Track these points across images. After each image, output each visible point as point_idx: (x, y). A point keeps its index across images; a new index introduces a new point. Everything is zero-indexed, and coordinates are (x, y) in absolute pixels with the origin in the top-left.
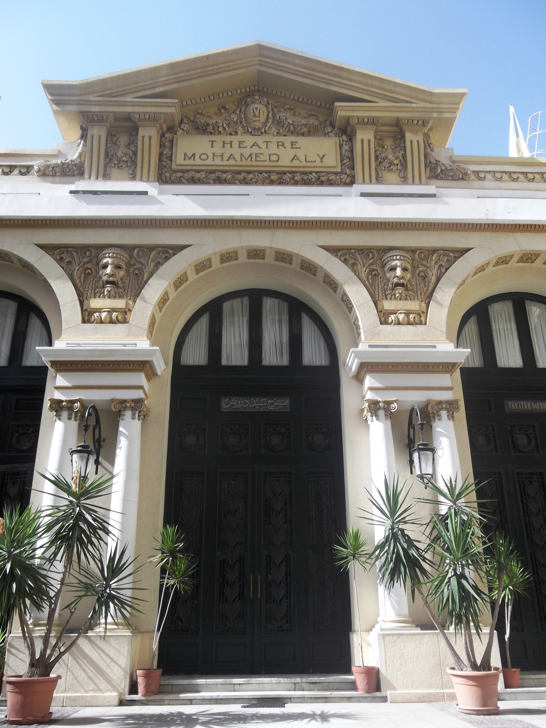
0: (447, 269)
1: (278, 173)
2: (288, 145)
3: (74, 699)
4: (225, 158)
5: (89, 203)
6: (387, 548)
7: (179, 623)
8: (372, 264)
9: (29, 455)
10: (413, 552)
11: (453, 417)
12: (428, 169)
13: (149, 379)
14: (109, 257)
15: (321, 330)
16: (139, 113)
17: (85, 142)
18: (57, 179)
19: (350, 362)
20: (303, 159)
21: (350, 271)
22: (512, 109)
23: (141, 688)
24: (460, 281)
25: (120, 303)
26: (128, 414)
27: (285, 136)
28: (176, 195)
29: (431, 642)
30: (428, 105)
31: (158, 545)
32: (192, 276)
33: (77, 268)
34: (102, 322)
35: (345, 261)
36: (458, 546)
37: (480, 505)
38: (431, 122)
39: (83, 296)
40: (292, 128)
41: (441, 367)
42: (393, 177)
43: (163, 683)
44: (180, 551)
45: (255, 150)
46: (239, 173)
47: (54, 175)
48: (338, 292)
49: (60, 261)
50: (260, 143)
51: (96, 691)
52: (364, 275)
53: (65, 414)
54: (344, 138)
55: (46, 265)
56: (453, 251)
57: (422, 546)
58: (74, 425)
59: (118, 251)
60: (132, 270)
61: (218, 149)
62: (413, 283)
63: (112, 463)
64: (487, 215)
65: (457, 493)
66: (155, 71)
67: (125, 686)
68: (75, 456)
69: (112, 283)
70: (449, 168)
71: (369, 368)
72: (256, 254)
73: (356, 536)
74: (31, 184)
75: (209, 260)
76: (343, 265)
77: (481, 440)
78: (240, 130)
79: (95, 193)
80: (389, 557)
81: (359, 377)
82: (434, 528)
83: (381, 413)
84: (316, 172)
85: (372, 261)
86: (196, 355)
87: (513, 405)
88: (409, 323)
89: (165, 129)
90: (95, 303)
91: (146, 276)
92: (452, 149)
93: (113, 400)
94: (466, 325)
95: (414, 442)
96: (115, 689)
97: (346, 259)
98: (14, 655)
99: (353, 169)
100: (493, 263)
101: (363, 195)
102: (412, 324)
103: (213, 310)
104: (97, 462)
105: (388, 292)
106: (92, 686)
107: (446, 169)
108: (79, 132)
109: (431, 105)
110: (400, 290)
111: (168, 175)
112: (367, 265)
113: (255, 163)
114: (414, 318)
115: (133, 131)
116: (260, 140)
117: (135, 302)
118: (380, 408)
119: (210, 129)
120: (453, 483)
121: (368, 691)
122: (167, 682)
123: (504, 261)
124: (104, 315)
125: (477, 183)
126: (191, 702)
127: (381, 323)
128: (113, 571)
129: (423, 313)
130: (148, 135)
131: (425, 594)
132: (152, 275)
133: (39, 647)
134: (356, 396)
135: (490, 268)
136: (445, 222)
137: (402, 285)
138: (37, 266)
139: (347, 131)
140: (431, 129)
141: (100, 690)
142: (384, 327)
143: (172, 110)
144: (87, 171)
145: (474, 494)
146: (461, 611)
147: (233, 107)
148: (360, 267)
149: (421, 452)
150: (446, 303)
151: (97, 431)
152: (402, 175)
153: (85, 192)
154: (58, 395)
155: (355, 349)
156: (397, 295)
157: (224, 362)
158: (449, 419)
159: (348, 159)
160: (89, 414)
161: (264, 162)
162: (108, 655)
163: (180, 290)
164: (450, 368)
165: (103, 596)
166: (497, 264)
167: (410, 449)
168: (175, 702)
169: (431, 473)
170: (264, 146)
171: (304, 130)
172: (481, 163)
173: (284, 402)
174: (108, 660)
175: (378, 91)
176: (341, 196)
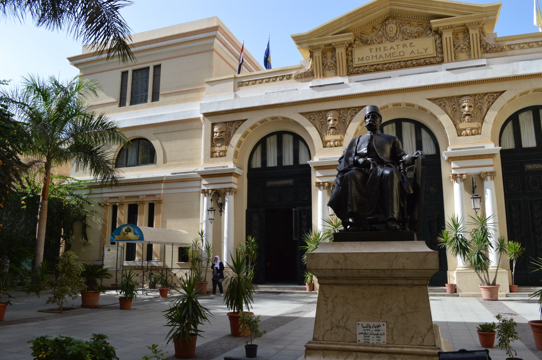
0: (492, 103)
2: (408, 45)
4: (378, 58)
5: (318, 91)
8: (454, 105)
12: (482, 49)
16: (335, 43)
17: (313, 59)
18: (303, 80)
19: (444, 156)
20: (416, 52)
24: (499, 109)
25: (338, 137)
27: (407, 39)
28: (357, 82)
30: (480, 14)
34: (331, 147)
38: (482, 23)
40: (410, 35)
42: (463, 55)
45: (392, 51)
46: (385, 64)
49: (310, 119)
50: (394, 46)
53: (322, 187)
54: (437, 36)
58: (326, 191)
61: (374, 53)
66: (340, 20)
69: (333, 128)
70: (493, 46)
79: (321, 86)
83: (459, 179)
84: (423, 58)
87: (529, 167)
88: (472, 135)
89: (348, 46)
90: (328, 138)
91: (348, 123)
94: (506, 127)
99: (443, 53)
101: (447, 70)
107: (492, 47)
108: (308, 54)
109: (482, 14)
110: (467, 118)
111: (352, 70)
113: (392, 58)
115: (334, 50)
116: (394, 44)
119: (369, 42)
125: (510, 53)
127: (459, 136)
130: (341, 51)
134: (448, 170)
137: (469, 115)
138: (301, 123)
139: (438, 33)
140: (484, 24)
142: (459, 137)
144: (315, 74)
150: (493, 118)
152: (468, 54)
153: (316, 86)
154: (318, 180)
155: (445, 152)
158: (491, 180)
159: (440, 48)
166: (521, 95)
170: (396, 48)
171: (416, 35)
172: (512, 40)
175: (453, 10)
176: (436, 71)
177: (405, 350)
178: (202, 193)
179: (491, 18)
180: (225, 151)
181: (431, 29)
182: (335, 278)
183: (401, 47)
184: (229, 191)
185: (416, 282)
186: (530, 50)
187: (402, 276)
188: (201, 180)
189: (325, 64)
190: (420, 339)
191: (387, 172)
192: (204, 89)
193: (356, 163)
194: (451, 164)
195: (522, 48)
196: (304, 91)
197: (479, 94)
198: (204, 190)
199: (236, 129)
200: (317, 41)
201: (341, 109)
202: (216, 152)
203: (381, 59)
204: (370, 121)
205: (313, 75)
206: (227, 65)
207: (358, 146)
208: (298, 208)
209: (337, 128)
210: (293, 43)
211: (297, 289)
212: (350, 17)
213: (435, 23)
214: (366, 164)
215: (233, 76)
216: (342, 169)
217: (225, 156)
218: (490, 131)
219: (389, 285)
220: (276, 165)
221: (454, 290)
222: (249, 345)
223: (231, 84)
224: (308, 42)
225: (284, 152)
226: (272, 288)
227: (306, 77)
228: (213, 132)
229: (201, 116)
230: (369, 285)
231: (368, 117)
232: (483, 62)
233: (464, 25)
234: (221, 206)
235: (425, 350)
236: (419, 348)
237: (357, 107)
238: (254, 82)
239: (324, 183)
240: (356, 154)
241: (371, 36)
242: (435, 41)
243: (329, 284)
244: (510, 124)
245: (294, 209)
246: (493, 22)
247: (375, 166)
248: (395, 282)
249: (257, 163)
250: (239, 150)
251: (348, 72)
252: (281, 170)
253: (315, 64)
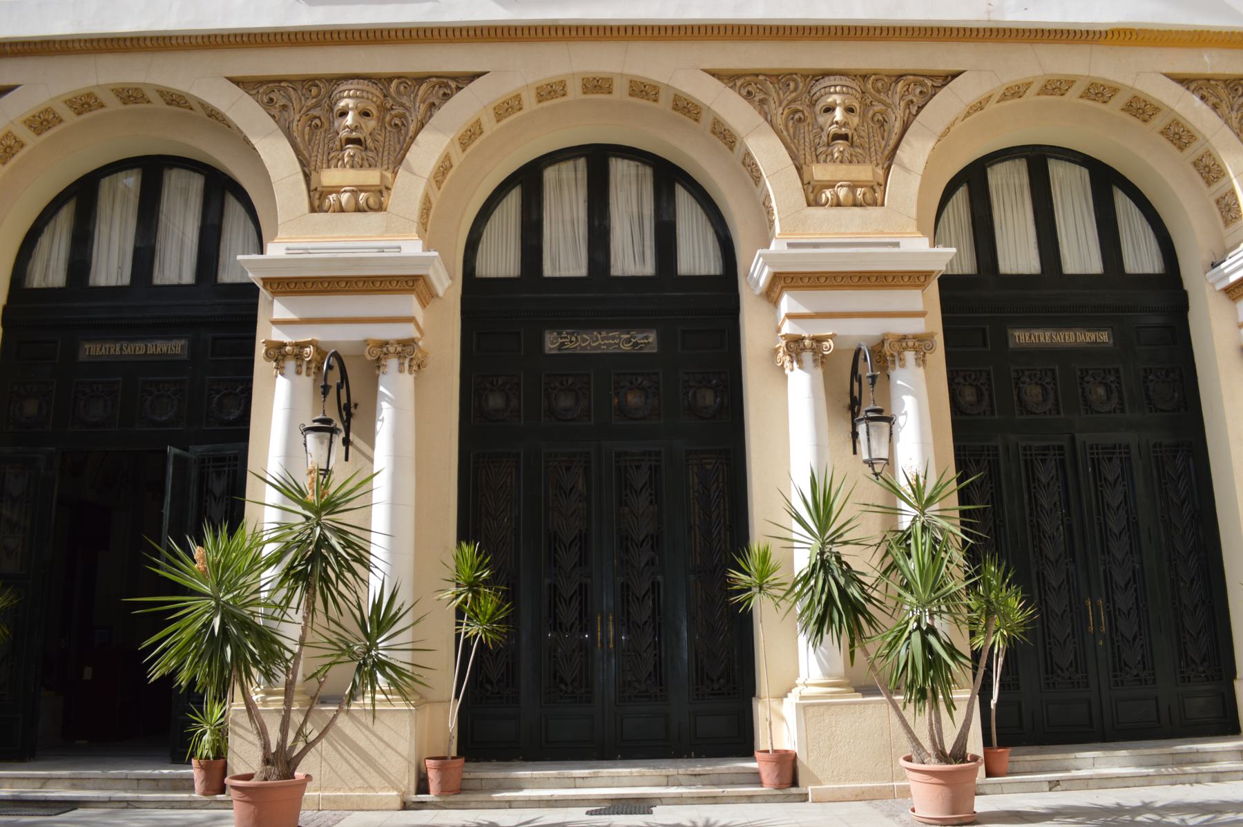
0: (920, 108)
3: (335, 800)
6: (812, 582)
7: (489, 687)
8: (794, 101)
9: (237, 430)
10: (854, 591)
11: (924, 361)
13: (424, 305)
14: (349, 97)
15: (707, 215)
21: (756, 113)
23: (434, 785)
24: (940, 129)
25: (371, 177)
26: (393, 363)
29: (876, 715)
31: (450, 574)
32: (490, 126)
33: (297, 118)
34: (342, 210)
36: (924, 586)
37: (963, 513)
39: (309, 165)
41: (906, 279)
43: (466, 776)
48: (736, 150)
51: (366, 789)
52: (779, 121)
53: (291, 365)
55: (245, 112)
56: (931, 77)
57: (868, 580)
58: (306, 382)
59: (363, 85)
60: (388, 118)
62: (863, 134)
63: (372, 446)
64: (989, 12)
65: (926, 496)
67: (410, 782)
69: (357, 141)
71: (789, 281)
72: (597, 85)
73: (765, 557)
75: (518, 97)
76: (745, 102)
77: (969, 395)
80: (816, 599)
81: (771, 295)
82: (887, 553)
83: (807, 357)
85: (794, 95)
86: (499, 258)
87: (1022, 337)
88: (855, 205)
90: (330, 177)
91: (412, 128)
93: (366, 342)
95: (860, 404)
96: (395, 788)
97: (749, 93)
98: (240, 736)
100: (997, 97)
102: (861, 206)
103: (528, 180)
104: (346, 442)
105: (820, 150)
106: (360, 782)
110: (840, 146)
112: (785, 103)
114: (864, 194)
117: (395, 173)
118: (804, 349)
120: (921, 480)
121: (780, 786)
122: (472, 775)
123: (1015, 92)
124: (345, 198)
126: (510, 804)
127: (809, 205)
128: (379, 624)
129: (880, 185)
131: (873, 656)
132: (423, 126)
133: (274, 737)
135: (992, 106)
136: (918, 25)
137: (845, 137)
138: (231, 115)
141: (371, 788)
145: (954, 498)
146: (927, 679)
148: (773, 106)
149: (871, 424)
151: (343, 392)
154: (278, 335)
155: (765, 251)
156: (836, 155)
157: (548, 271)
158: (918, 365)
160: (330, 367)
162: (380, 739)
163: (469, 150)
164: (922, 279)
165: (365, 664)
166: (1004, 97)
167: (854, 415)
168: (485, 805)
169: (885, 455)
173: (647, 338)
174: (381, 746)
194: (775, 303)
201: (390, 79)
209: (369, 143)
218: (915, 198)
220: (126, 280)
221: (789, 773)
226: (45, 781)
239: (301, 346)
244: (961, 195)
245: (172, 450)
249: (50, 270)
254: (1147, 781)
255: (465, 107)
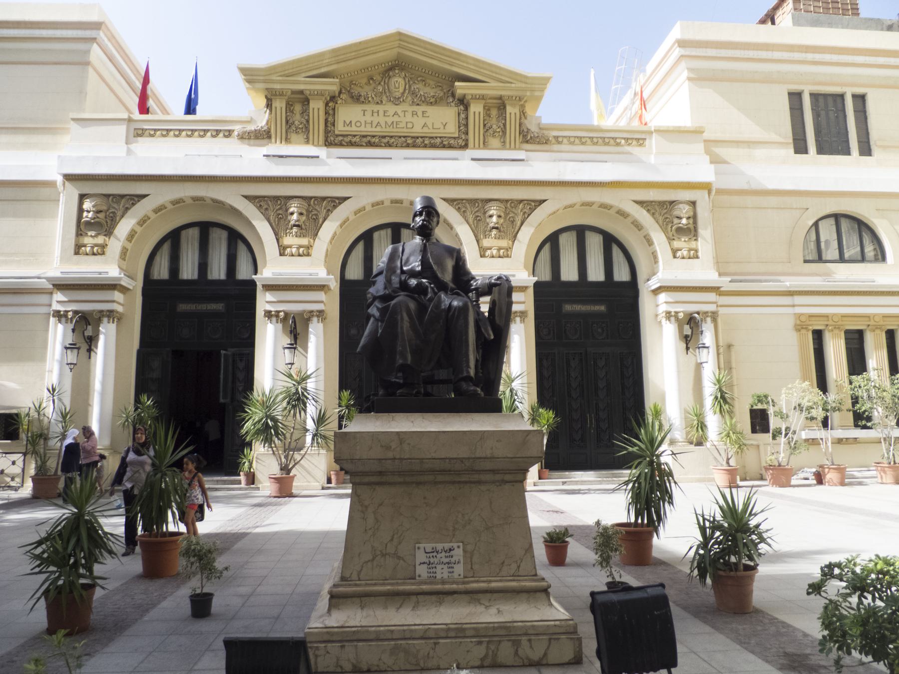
0: (529, 215)
1: (413, 137)
2: (420, 114)
4: (374, 125)
16: (310, 90)
17: (271, 111)
18: (252, 142)
20: (430, 127)
22: (592, 72)
25: (304, 241)
26: (315, 319)
30: (524, 85)
34: (293, 255)
35: (459, 209)
42: (495, 142)
44: (353, 405)
45: (396, 119)
46: (384, 137)
47: (249, 138)
49: (260, 207)
50: (399, 112)
52: (471, 221)
53: (274, 319)
54: (462, 107)
55: (250, 210)
58: (280, 325)
61: (368, 118)
63: (306, 352)
66: (321, 55)
68: (287, 351)
69: (298, 226)
74: (233, 146)
78: (384, 98)
79: (281, 157)
87: (568, 308)
88: (500, 257)
90: (287, 240)
91: (321, 221)
92: (540, 117)
93: (304, 311)
99: (467, 134)
101: (473, 159)
103: (367, 238)
108: (264, 101)
110: (494, 232)
113: (395, 130)
115: (306, 101)
116: (399, 109)
119: (362, 99)
125: (556, 147)
130: (317, 106)
135: (561, 211)
137: (497, 228)
140: (526, 101)
142: (483, 259)
143: (335, 88)
147: (379, 78)
153: (274, 156)
154: (269, 307)
159: (464, 126)
161: (402, 130)
170: (402, 114)
171: (432, 100)
172: (561, 130)
177: (493, 585)
178: (54, 316)
179: (537, 94)
180: (103, 246)
181: (453, 95)
182: (381, 473)
183: (409, 115)
184: (109, 317)
185: (508, 477)
186: (582, 148)
187: (488, 468)
188: (51, 293)
189: (291, 121)
190: (514, 566)
191: (455, 303)
192: (66, 131)
193: (404, 286)
195: (572, 143)
196: (252, 161)
197: (512, 201)
198: (59, 311)
199: (127, 209)
200: (280, 82)
201: (311, 198)
202: (85, 246)
203: (379, 129)
204: (423, 220)
205: (269, 137)
206: (112, 95)
207: (404, 258)
208: (231, 351)
210: (239, 78)
211: (225, 482)
212: (337, 53)
213: (461, 87)
214: (421, 290)
215: (125, 116)
216: (381, 293)
217: (103, 253)
219: (466, 482)
220: (196, 277)
222: (198, 595)
223: (122, 129)
224: (265, 82)
225: (210, 257)
227: (257, 138)
228: (81, 210)
229: (59, 179)
230: (436, 483)
231: (421, 214)
232: (520, 154)
233: (500, 98)
234: (91, 342)
235: (523, 584)
236: (514, 580)
237: (338, 198)
238: (164, 133)
239: (278, 312)
240: (403, 272)
241: (366, 91)
242: (459, 114)
243: (369, 484)
244: (547, 247)
245: (223, 352)
246: (539, 99)
247: (436, 294)
248: (476, 477)
249: (162, 271)
250: (129, 246)
251: (326, 140)
252: (202, 287)
253: (273, 119)
254: (600, 483)
255: (343, 211)
